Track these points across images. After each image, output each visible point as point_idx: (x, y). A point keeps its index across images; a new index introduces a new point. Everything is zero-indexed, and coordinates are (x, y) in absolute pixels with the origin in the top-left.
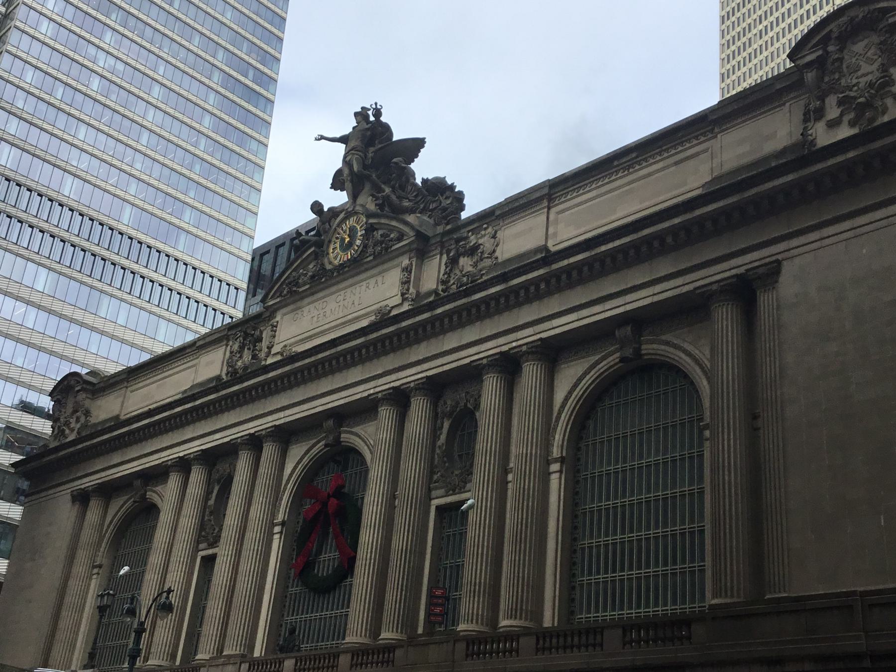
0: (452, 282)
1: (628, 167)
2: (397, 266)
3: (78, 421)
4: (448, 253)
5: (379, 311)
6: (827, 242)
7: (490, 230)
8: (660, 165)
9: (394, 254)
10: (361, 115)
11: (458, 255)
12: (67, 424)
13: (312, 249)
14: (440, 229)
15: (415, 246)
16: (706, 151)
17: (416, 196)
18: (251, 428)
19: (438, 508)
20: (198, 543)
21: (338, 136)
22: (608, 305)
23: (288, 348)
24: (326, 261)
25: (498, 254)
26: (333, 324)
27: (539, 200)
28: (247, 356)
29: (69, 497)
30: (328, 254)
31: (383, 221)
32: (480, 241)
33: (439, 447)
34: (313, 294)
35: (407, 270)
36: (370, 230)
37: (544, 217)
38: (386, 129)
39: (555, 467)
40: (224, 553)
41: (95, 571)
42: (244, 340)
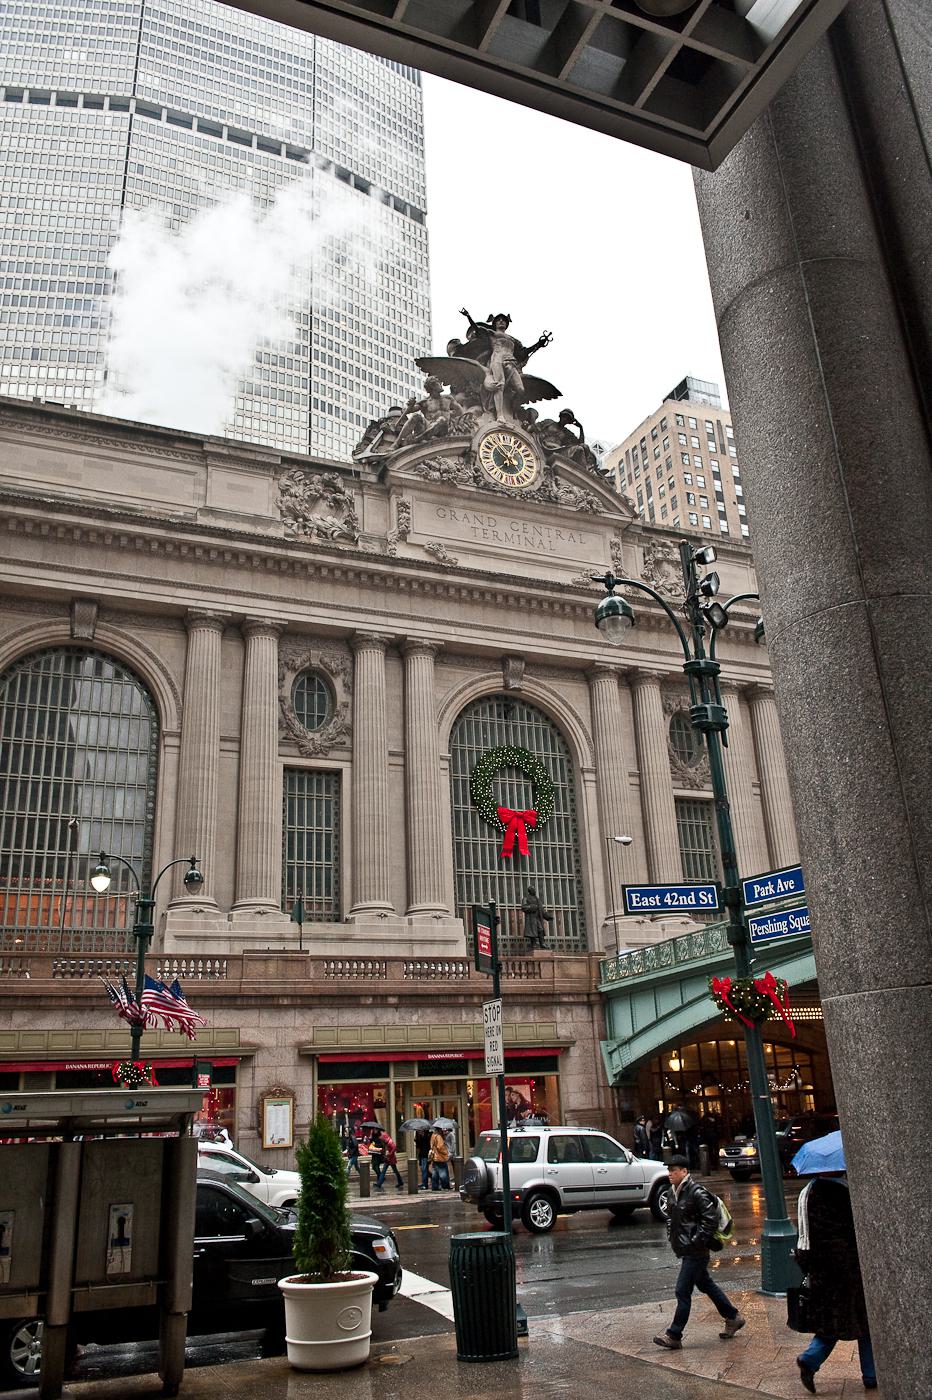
0: (661, 583)
13: (467, 445)
18: (398, 627)
34: (469, 499)
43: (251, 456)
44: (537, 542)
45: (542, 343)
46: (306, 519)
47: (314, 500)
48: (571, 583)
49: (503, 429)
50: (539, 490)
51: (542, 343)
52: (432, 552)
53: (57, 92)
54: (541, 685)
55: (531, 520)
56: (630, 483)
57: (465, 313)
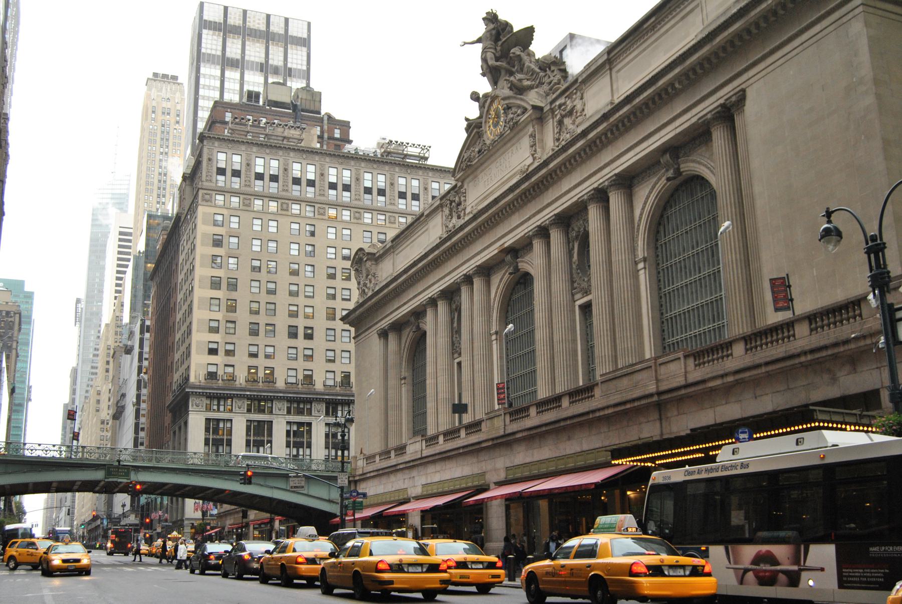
2: (525, 135)
3: (370, 282)
5: (522, 172)
7: (579, 94)
8: (672, 22)
9: (523, 125)
11: (563, 117)
12: (365, 285)
14: (550, 99)
15: (533, 117)
19: (580, 306)
20: (453, 354)
21: (475, 39)
25: (586, 112)
27: (602, 66)
28: (454, 220)
29: (376, 335)
35: (533, 136)
37: (608, 77)
38: (507, 26)
39: (641, 265)
40: (465, 359)
41: (403, 382)
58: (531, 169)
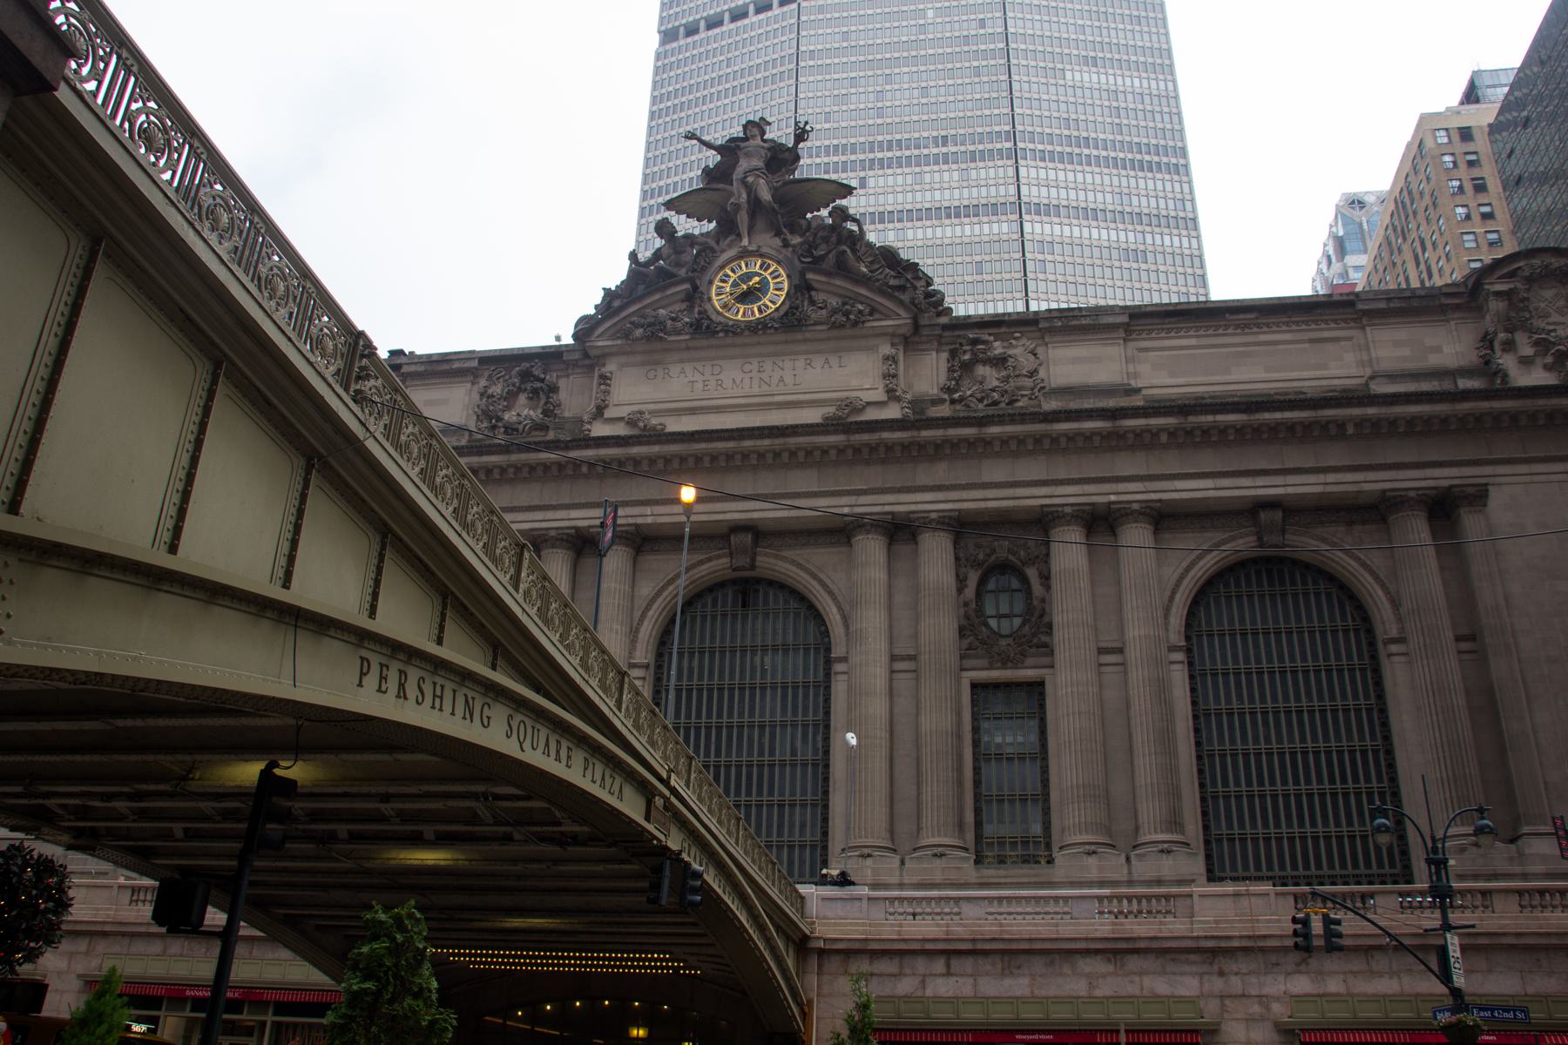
1: (1247, 326)
4: (953, 354)
6: (1536, 478)
10: (756, 127)
11: (975, 361)
13: (687, 286)
15: (903, 331)
16: (1350, 339)
17: (872, 262)
22: (1260, 481)
23: (647, 416)
24: (708, 307)
25: (1042, 374)
26: (742, 401)
30: (710, 299)
31: (838, 282)
32: (1010, 352)
33: (966, 604)
34: (688, 348)
36: (801, 288)
42: (522, 382)
43: (446, 367)
44: (775, 380)
45: (801, 135)
46: (499, 419)
47: (511, 396)
48: (818, 420)
49: (745, 254)
50: (786, 314)
51: (801, 135)
52: (631, 423)
53: (730, 10)
54: (784, 559)
55: (769, 355)
56: (1405, 239)
57: (691, 136)
58: (871, 415)
